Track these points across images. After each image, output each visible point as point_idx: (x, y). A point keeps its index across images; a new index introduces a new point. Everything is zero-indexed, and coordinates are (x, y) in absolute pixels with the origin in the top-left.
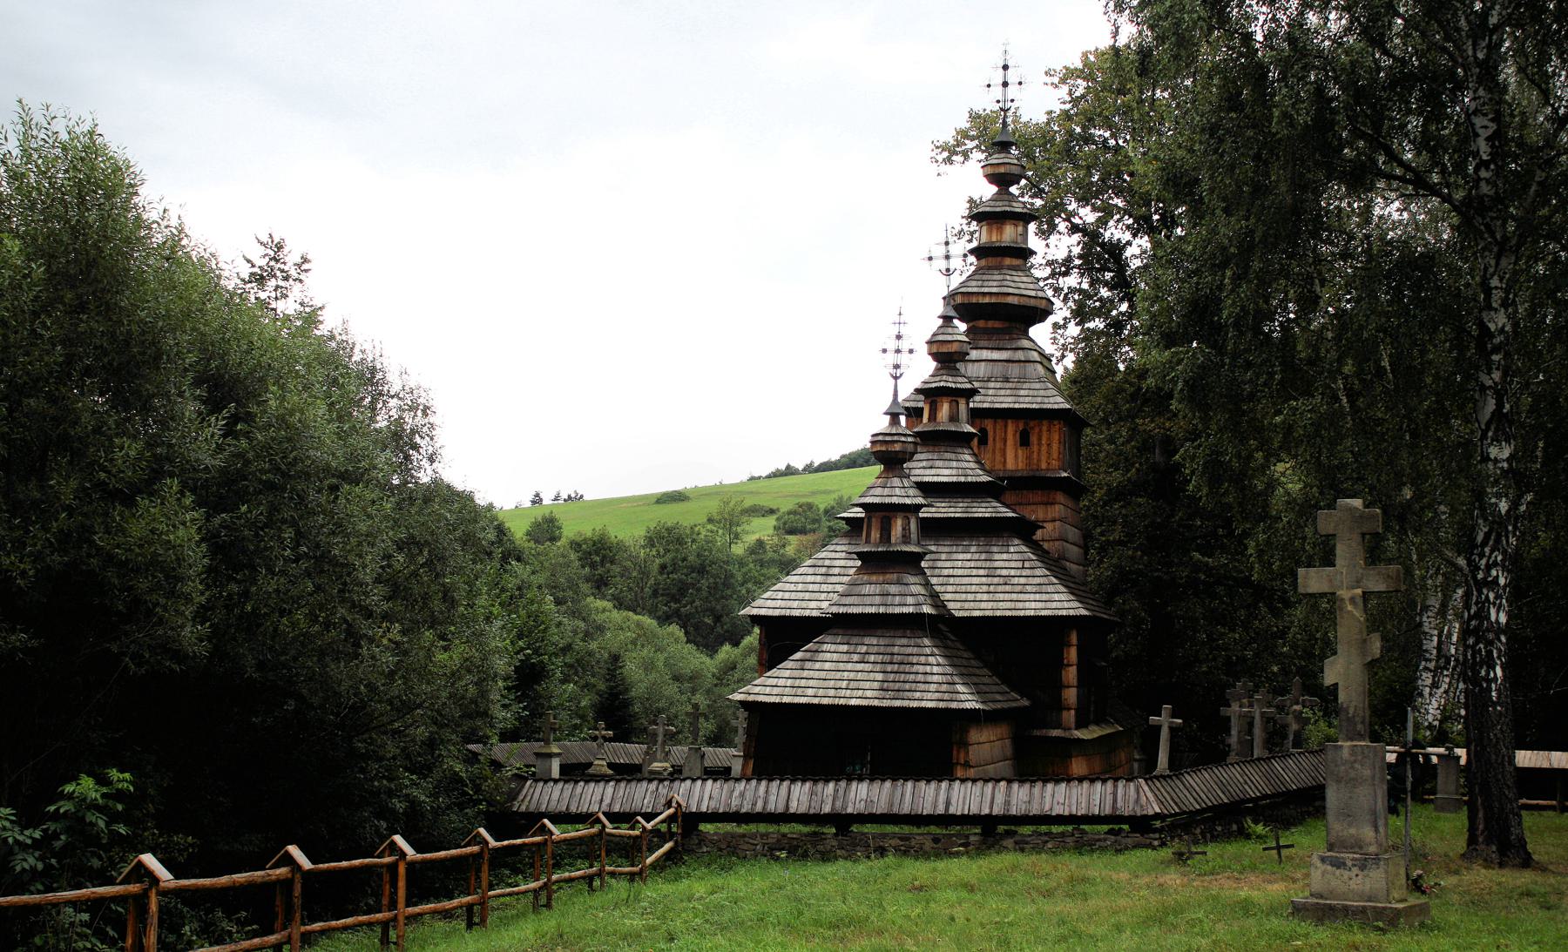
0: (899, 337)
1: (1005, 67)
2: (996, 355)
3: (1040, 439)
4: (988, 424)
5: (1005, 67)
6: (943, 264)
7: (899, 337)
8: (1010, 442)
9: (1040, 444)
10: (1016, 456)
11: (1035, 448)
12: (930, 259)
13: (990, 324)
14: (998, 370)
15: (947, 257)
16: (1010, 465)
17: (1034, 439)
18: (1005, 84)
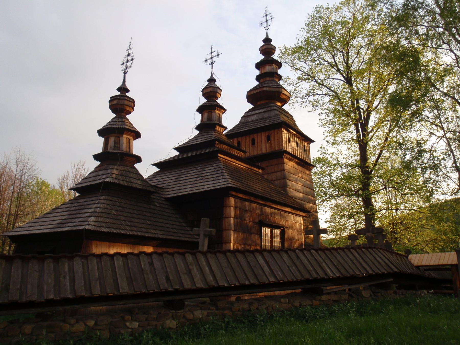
0: (128, 55)
1: (266, 15)
2: (260, 111)
3: (275, 138)
4: (255, 136)
5: (266, 15)
6: (209, 61)
7: (128, 55)
8: (263, 141)
9: (274, 140)
10: (266, 147)
11: (273, 142)
12: (206, 61)
13: (262, 102)
14: (260, 116)
15: (212, 58)
16: (264, 151)
17: (272, 138)
18: (267, 21)
